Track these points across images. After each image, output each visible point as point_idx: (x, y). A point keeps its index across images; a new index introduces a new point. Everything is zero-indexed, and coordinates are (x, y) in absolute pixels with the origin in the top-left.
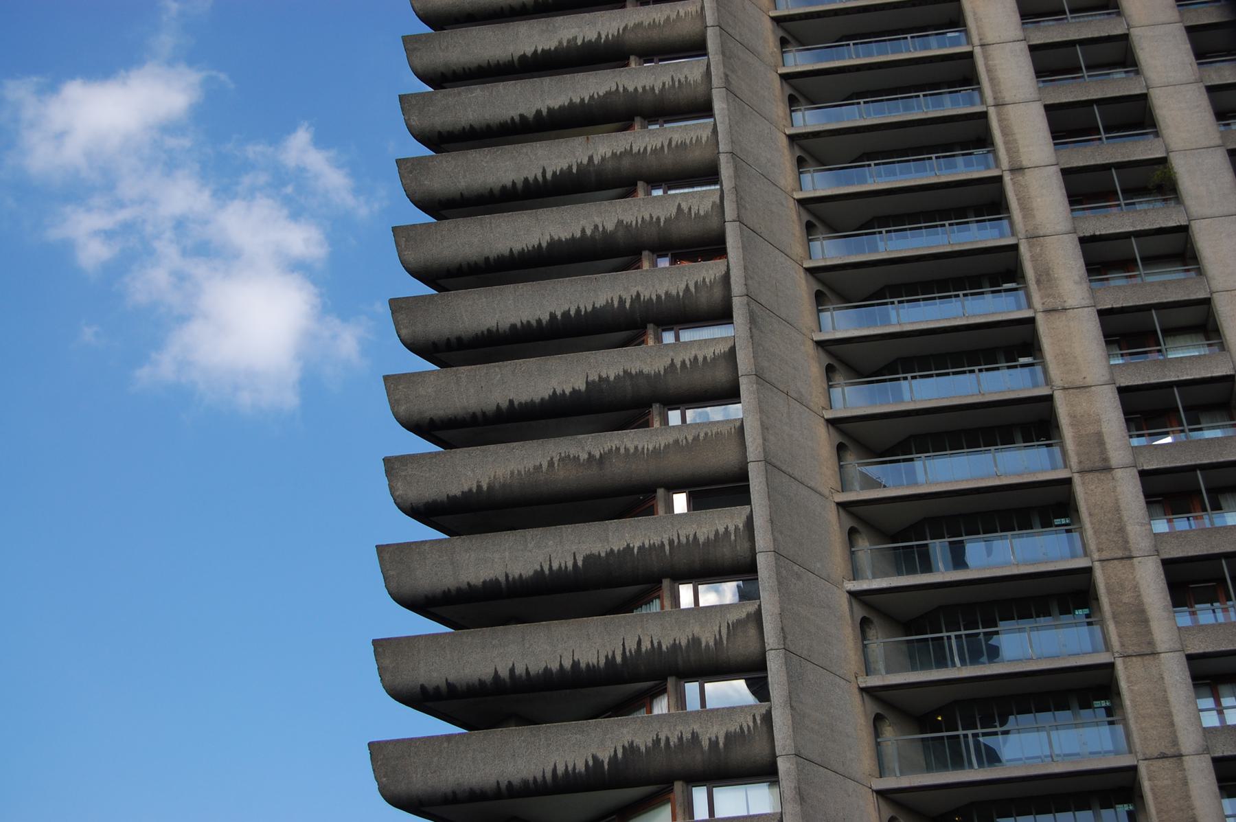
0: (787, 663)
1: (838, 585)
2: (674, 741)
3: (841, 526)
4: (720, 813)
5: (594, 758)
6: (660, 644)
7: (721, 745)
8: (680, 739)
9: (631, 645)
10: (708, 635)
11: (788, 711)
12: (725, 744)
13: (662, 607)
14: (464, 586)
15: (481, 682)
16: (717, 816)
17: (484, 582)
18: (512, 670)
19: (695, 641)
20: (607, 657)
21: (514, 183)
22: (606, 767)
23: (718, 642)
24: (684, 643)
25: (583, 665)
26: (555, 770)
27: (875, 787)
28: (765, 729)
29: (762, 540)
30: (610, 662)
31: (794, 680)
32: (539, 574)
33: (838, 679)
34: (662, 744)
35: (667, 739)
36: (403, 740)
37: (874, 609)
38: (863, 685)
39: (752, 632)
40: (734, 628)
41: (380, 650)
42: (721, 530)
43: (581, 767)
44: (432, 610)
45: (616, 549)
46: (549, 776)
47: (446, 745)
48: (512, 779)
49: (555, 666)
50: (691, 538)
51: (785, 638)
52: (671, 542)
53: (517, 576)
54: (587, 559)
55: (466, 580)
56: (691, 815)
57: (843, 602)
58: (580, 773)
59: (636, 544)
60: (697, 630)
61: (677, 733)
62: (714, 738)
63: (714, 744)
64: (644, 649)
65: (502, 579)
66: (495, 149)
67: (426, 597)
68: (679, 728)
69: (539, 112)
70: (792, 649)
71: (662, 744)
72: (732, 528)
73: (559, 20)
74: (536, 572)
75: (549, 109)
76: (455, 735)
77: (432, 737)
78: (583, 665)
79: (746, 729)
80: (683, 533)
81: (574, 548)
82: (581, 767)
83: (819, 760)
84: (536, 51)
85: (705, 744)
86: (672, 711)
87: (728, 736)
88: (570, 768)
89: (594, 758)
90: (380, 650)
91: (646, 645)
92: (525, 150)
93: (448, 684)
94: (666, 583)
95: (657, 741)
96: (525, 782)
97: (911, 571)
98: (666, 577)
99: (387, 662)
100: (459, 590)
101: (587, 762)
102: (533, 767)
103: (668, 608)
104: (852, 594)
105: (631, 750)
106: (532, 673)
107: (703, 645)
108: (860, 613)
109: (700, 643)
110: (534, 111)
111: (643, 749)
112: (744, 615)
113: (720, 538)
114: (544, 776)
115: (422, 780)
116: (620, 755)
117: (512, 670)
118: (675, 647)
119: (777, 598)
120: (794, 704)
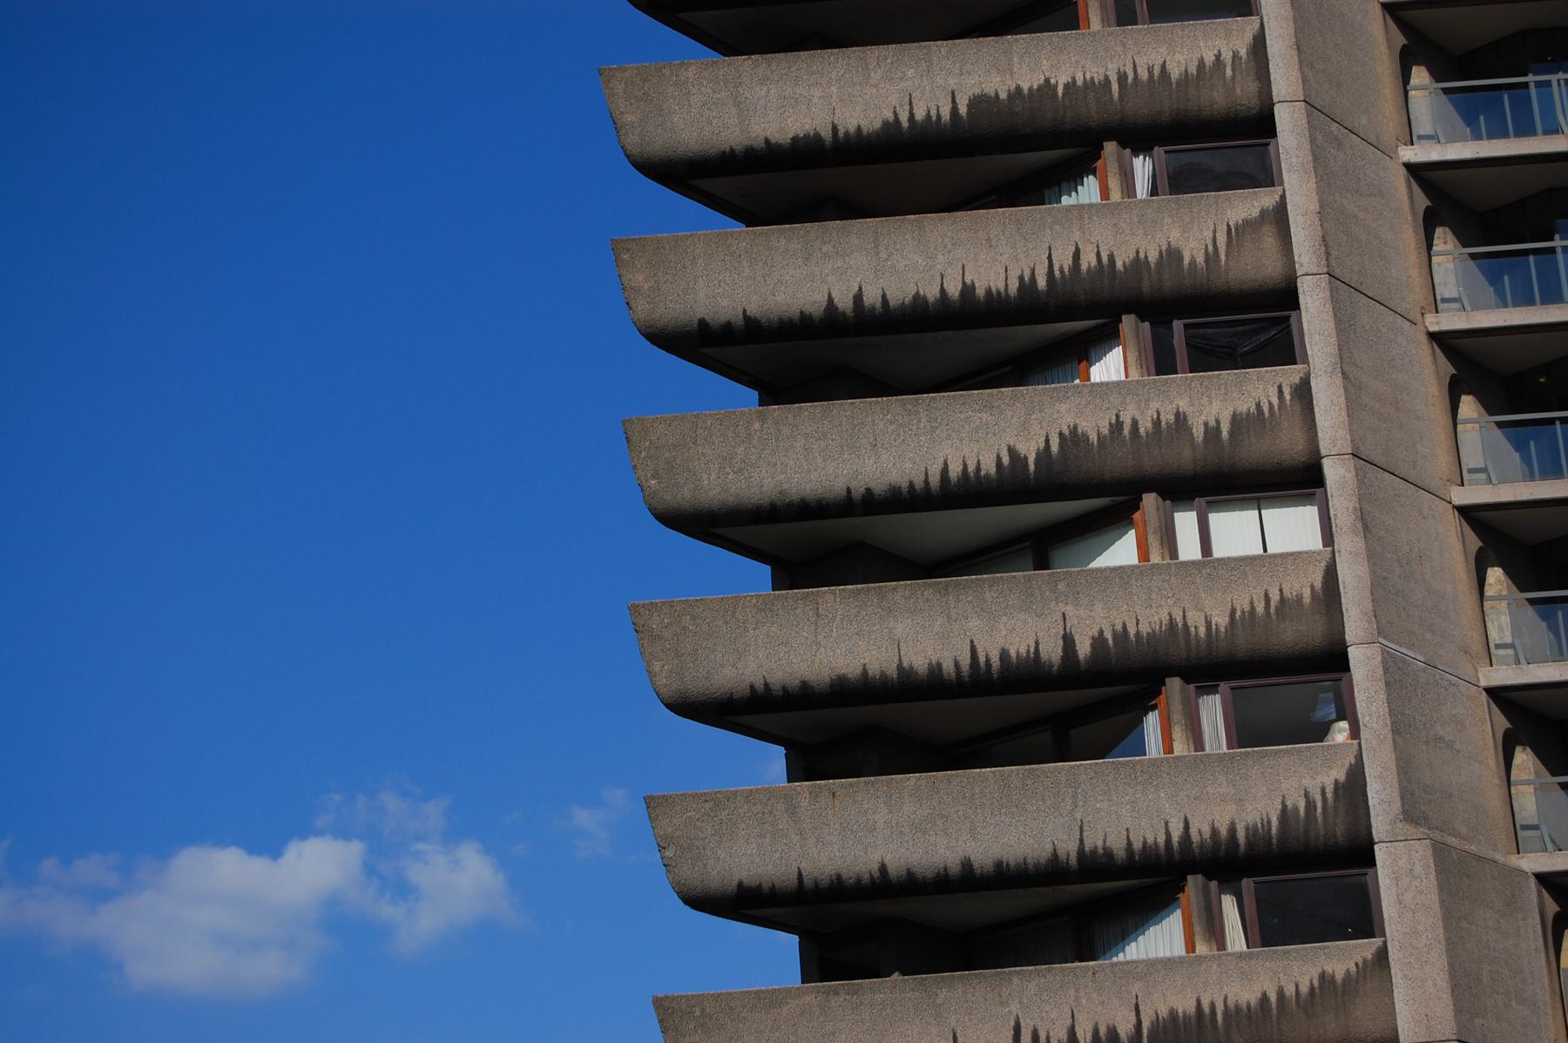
1: (1390, 154)
2: (1145, 426)
3: (1390, 47)
5: (1011, 451)
6: (1111, 258)
7: (1225, 434)
8: (1157, 423)
9: (1063, 260)
11: (1339, 380)
12: (1232, 433)
13: (1105, 193)
14: (759, 143)
16: (1219, 551)
17: (795, 139)
18: (858, 298)
19: (1172, 256)
20: (1021, 278)
22: (1032, 467)
23: (1211, 258)
24: (1153, 257)
25: (980, 292)
26: (945, 471)
27: (1457, 501)
28: (1298, 409)
29: (1284, 80)
30: (1027, 287)
31: (1344, 325)
32: (892, 127)
33: (1399, 320)
34: (1126, 431)
35: (1135, 423)
37: (1448, 199)
38: (1433, 328)
39: (1270, 241)
40: (1239, 234)
42: (1209, 58)
43: (989, 467)
44: (703, 184)
45: (1025, 87)
46: (935, 480)
47: (757, 426)
48: (872, 485)
49: (932, 293)
50: (1157, 72)
51: (1328, 254)
52: (1122, 78)
53: (852, 130)
54: (975, 102)
56: (1173, 551)
57: (1400, 178)
58: (987, 476)
59: (1061, 80)
60: (1175, 236)
61: (1151, 413)
62: (1212, 423)
63: (1212, 432)
64: (1084, 267)
65: (826, 134)
68: (1154, 405)
70: (1338, 272)
71: (1126, 431)
72: (1227, 56)
74: (886, 123)
78: (980, 292)
79: (1266, 409)
80: (1142, 62)
81: (952, 83)
82: (989, 467)
85: (1198, 432)
86: (1135, 375)
87: (1236, 419)
88: (971, 468)
89: (1011, 451)
91: (1088, 260)
94: (1110, 147)
95: (1117, 426)
99: (638, 279)
101: (999, 459)
102: (908, 465)
103: (1116, 196)
104: (1414, 170)
105: (1073, 439)
107: (1186, 261)
109: (1180, 258)
111: (1094, 438)
112: (1255, 213)
113: (1206, 73)
114: (926, 482)
116: (1055, 448)
117: (858, 298)
118: (1138, 264)
119: (1312, 184)
120: (1347, 368)
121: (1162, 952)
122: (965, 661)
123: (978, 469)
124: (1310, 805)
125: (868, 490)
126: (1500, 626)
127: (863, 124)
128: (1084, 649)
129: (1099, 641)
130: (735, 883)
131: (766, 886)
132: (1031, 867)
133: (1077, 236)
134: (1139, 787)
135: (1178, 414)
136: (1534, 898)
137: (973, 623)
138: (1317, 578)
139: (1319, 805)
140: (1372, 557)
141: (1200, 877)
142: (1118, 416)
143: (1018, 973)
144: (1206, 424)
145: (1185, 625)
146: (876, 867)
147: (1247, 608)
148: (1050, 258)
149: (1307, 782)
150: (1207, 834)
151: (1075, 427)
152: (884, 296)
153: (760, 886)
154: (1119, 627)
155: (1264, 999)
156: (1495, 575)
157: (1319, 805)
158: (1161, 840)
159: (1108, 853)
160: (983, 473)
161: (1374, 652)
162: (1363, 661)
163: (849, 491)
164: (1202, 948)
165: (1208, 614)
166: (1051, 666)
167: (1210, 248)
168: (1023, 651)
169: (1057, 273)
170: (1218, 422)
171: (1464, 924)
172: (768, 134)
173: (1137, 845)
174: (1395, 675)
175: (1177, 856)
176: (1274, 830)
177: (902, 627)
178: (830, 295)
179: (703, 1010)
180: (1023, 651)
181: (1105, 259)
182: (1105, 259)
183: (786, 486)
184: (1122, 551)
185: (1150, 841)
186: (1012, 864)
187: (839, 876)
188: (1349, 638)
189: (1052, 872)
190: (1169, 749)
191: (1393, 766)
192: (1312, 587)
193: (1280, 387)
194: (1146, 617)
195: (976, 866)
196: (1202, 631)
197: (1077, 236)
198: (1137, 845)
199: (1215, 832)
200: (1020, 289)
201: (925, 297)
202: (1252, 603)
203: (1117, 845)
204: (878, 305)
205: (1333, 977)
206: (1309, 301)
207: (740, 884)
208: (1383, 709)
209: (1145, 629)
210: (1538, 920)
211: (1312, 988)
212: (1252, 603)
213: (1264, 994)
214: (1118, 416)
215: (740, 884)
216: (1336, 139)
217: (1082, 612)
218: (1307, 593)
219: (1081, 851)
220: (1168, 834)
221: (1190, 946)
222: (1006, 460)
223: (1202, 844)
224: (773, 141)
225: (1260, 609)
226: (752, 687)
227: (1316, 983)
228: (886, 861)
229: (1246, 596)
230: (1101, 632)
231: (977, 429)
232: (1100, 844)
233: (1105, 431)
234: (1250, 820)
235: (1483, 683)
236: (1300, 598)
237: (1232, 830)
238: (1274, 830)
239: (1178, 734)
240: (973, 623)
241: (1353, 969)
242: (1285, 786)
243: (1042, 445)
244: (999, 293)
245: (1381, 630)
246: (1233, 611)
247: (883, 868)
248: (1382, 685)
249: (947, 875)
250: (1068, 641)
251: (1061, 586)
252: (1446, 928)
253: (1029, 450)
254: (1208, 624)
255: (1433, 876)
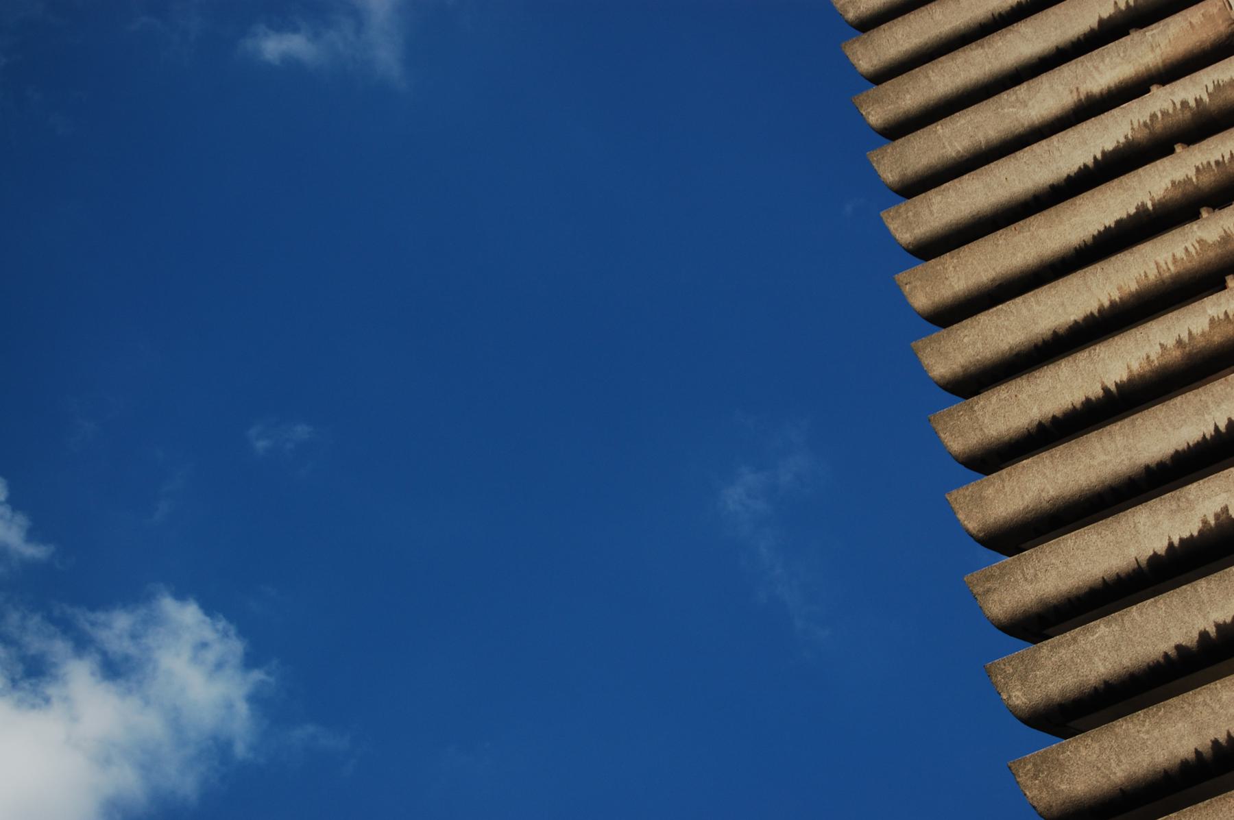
21: (1197, 751)
66: (1154, 708)
69: (1204, 635)
73: (1193, 490)
75: (1218, 626)
84: (1171, 545)
92: (1200, 699)
110: (1195, 635)
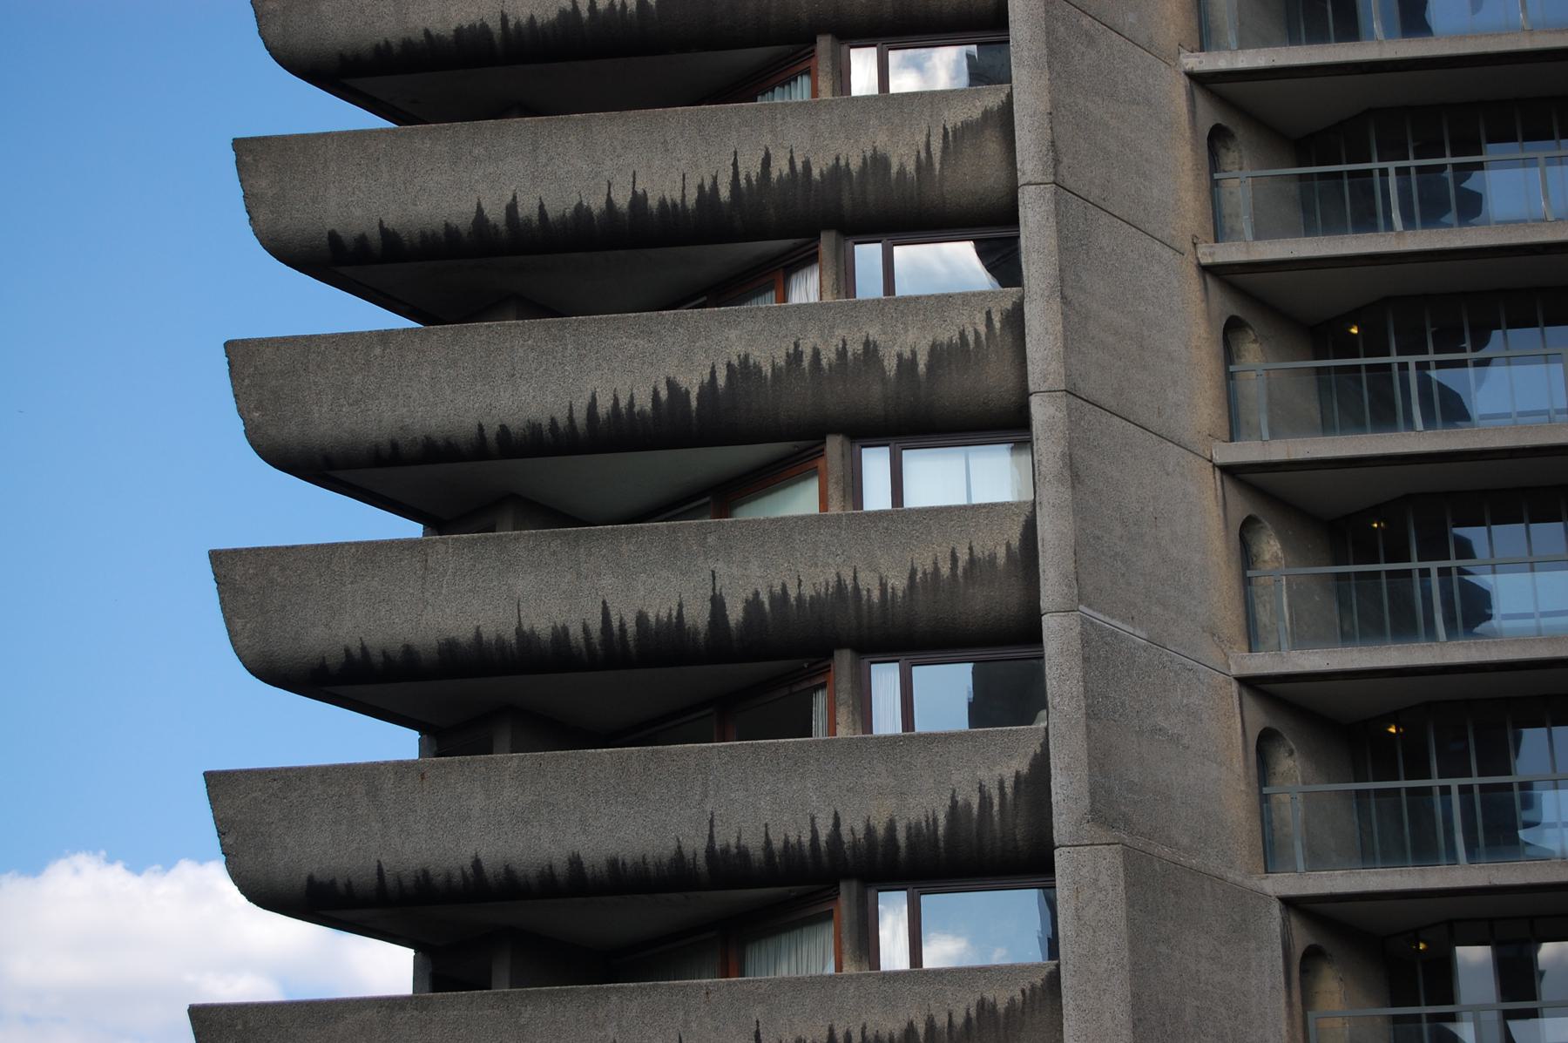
0: (1060, 213)
1: (1170, 60)
2: (828, 356)
4: (915, 498)
5: (671, 384)
7: (922, 367)
8: (842, 353)
9: (750, 166)
10: (903, 150)
11: (1056, 305)
12: (930, 367)
13: (815, 92)
14: (418, 36)
15: (451, 231)
18: (512, 208)
19: (878, 162)
20: (701, 187)
22: (694, 403)
23: (924, 166)
24: (855, 164)
25: (653, 203)
27: (1219, 459)
30: (708, 198)
31: (1071, 245)
33: (1157, 247)
35: (816, 353)
36: (295, 339)
37: (1238, 111)
40: (956, 139)
41: (249, 159)
43: (644, 402)
46: (581, 416)
47: (378, 351)
48: (508, 421)
49: (597, 203)
51: (1057, 162)
53: (524, 21)
55: (421, 26)
57: (1178, 91)
58: (642, 412)
60: (882, 141)
61: (836, 342)
62: (907, 354)
63: (907, 365)
64: (775, 175)
65: (495, 25)
67: (342, 57)
68: (840, 332)
70: (1070, 183)
74: (563, 13)
76: (398, 332)
77: (352, 334)
79: (971, 338)
82: (644, 402)
83: (1111, 403)
85: (890, 365)
86: (828, 299)
87: (935, 351)
88: (623, 403)
89: (671, 384)
90: (249, 159)
91: (780, 167)
93: (384, 231)
94: (824, 44)
95: (795, 357)
96: (534, 428)
97: (1317, 35)
98: (825, 32)
100: (407, 45)
101: (656, 393)
102: (550, 399)
103: (826, 94)
104: (1199, 80)
105: (743, 371)
106: (551, 215)
107: (894, 169)
108: (1209, 116)
111: (767, 370)
112: (976, 114)
114: (571, 418)
115: (331, 419)
116: (721, 381)
117: (512, 208)
118: (838, 173)
120: (1068, 292)
121: (814, 971)
122: (596, 625)
123: (631, 404)
124: (985, 801)
125: (503, 428)
126: (1277, 606)
127: (536, 14)
128: (735, 613)
129: (753, 605)
130: (304, 877)
131: (340, 883)
132: (652, 868)
133: (767, 139)
134: (782, 775)
135: (867, 343)
136: (1276, 925)
137: (607, 581)
138: (1014, 534)
139: (996, 801)
140: (1080, 511)
141: (854, 884)
142: (796, 345)
143: (618, 990)
144: (900, 356)
145: (856, 588)
146: (468, 862)
147: (929, 569)
148: (735, 164)
149: (982, 774)
150: (860, 835)
151: (747, 357)
152: (541, 206)
153: (333, 882)
154: (778, 589)
155: (910, 1030)
156: (1270, 548)
157: (996, 801)
158: (806, 839)
159: (743, 853)
160: (636, 409)
161: (1072, 621)
162: (1058, 633)
163: (481, 427)
164: (849, 969)
165: (883, 575)
166: (697, 632)
167: (923, 155)
168: (664, 614)
169: (743, 182)
170: (914, 353)
171: (1163, 948)
172: (428, 25)
173: (778, 844)
174: (1096, 650)
175: (825, 859)
176: (941, 830)
177: (523, 584)
178: (479, 205)
179: (245, 1023)
180: (664, 614)
181: (799, 166)
182: (799, 166)
183: (408, 421)
184: (802, 500)
185: (793, 839)
186: (629, 861)
187: (425, 873)
188: (1045, 604)
189: (675, 877)
190: (832, 728)
191: (1084, 757)
192: (1008, 546)
193: (989, 313)
194: (809, 576)
195: (586, 864)
196: (876, 594)
197: (767, 139)
198: (778, 844)
199: (870, 830)
200: (698, 201)
201: (588, 208)
202: (935, 563)
203: (754, 843)
204: (535, 217)
205: (994, 1005)
206: (1030, 214)
207: (311, 879)
208: (1078, 689)
209: (808, 592)
210: (1279, 952)
211: (968, 1019)
212: (935, 563)
213: (911, 1024)
214: (796, 345)
215: (311, 879)
216: (1087, 34)
217: (735, 570)
218: (1001, 552)
219: (710, 849)
220: (814, 832)
221: (839, 967)
222: (664, 394)
223: (855, 844)
224: (434, 33)
225: (945, 570)
226: (347, 651)
227: (973, 1013)
228: (481, 856)
229: (929, 556)
230: (757, 594)
231: (632, 357)
232: (733, 842)
233: (781, 362)
234: (913, 817)
235: (1234, 671)
236: (993, 558)
237: (891, 828)
238: (941, 830)
239: (843, 716)
240: (607, 581)
241: (1019, 997)
242: (956, 777)
243: (707, 378)
244: (675, 205)
245: (1081, 595)
246: (913, 572)
247: (477, 863)
248: (1078, 660)
249: (552, 874)
250: (717, 604)
251: (711, 540)
252: (1132, 951)
253: (692, 383)
254: (883, 587)
255: (1121, 888)
